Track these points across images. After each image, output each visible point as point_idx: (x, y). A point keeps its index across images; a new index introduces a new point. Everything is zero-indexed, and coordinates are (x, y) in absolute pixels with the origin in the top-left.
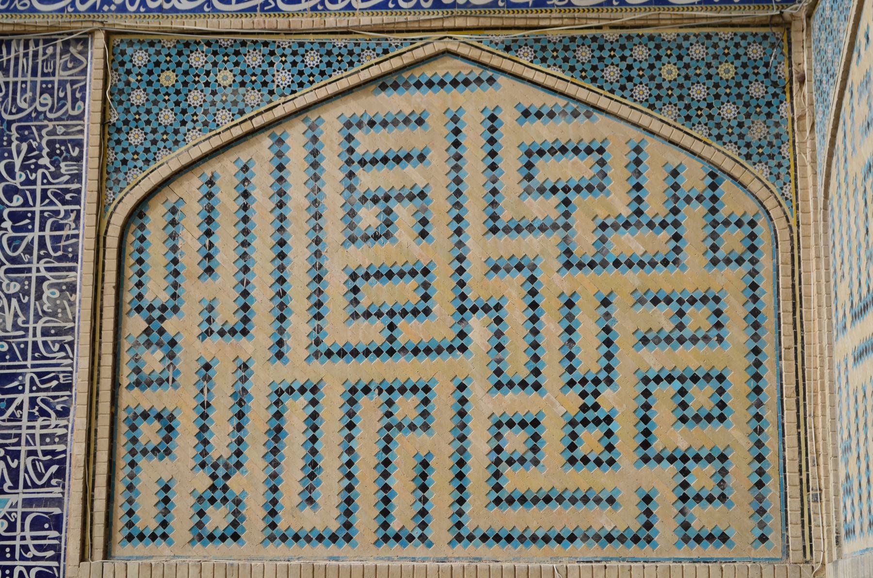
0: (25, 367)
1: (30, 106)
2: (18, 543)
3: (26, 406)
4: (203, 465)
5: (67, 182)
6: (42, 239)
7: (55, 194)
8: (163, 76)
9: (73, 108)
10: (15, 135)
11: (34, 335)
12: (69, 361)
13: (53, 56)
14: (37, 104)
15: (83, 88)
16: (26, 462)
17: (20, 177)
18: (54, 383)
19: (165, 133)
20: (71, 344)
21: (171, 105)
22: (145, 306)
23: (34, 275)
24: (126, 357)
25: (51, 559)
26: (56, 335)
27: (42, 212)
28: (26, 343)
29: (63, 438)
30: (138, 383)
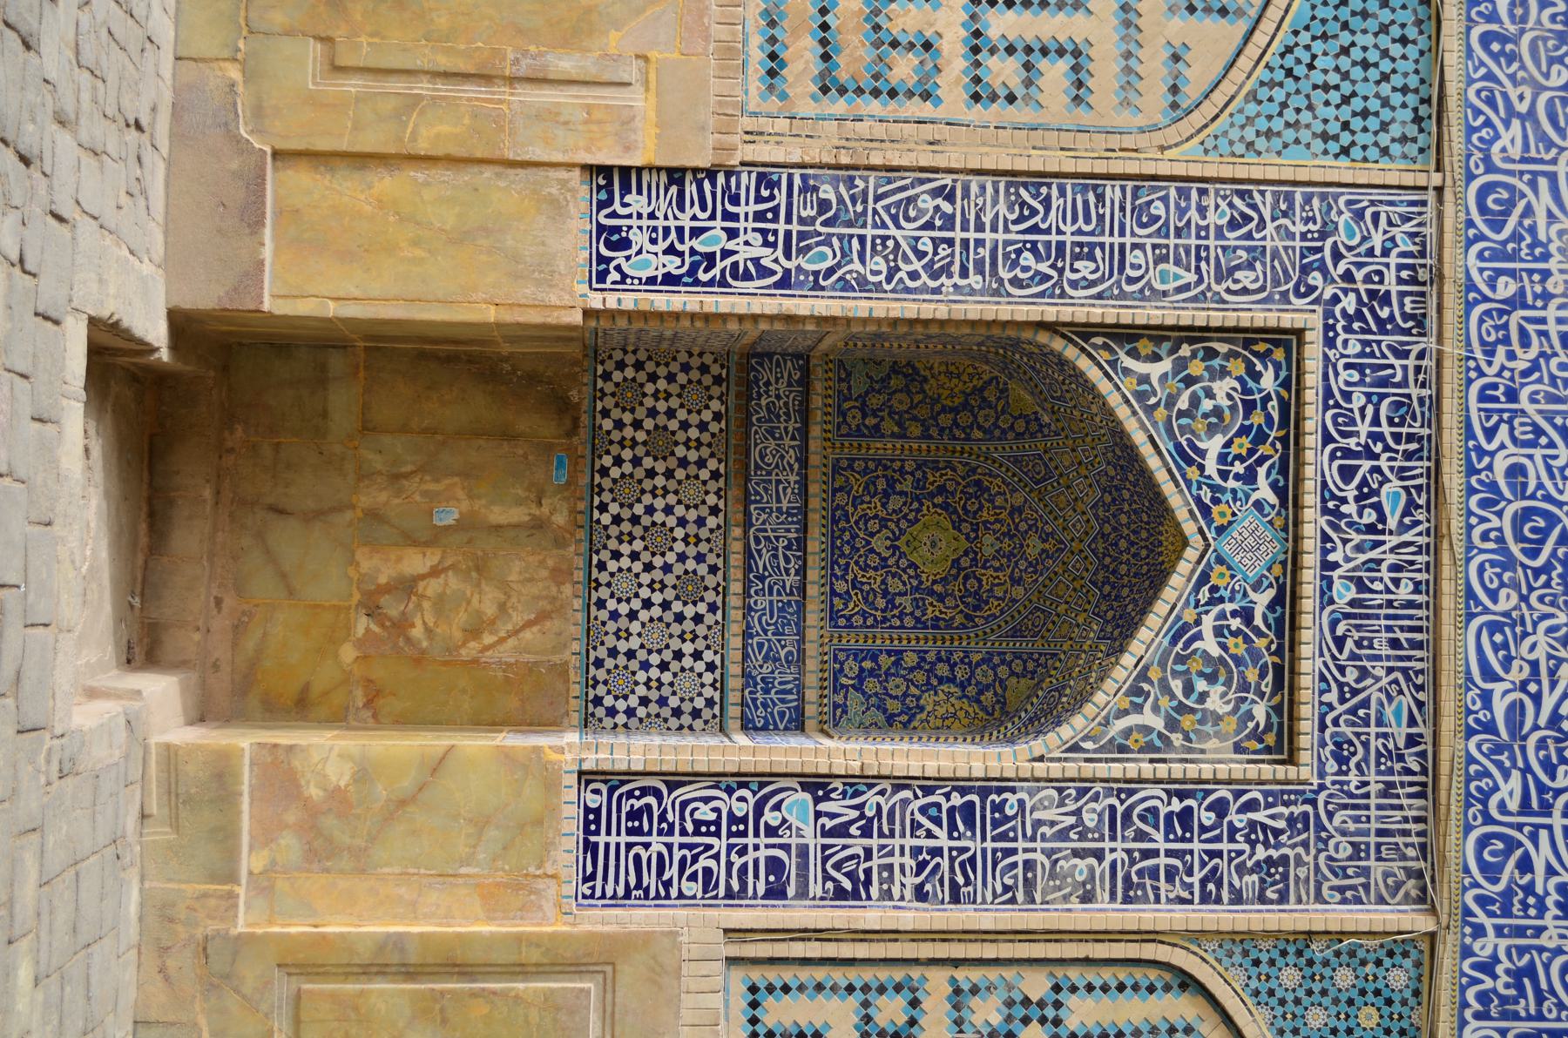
0: (984, 839)
1: (1336, 829)
2: (750, 840)
3: (932, 843)
5: (1231, 884)
6: (1155, 853)
7: (1215, 869)
8: (1373, 1011)
9: (1332, 888)
10: (1297, 810)
11: (1026, 850)
12: (989, 898)
13: (1404, 858)
14: (1338, 838)
15: (1359, 901)
16: (857, 845)
17: (1239, 820)
18: (960, 880)
19: (1294, 1016)
20: (1013, 901)
21: (1333, 1023)
22: (1060, 997)
23: (1107, 845)
24: (993, 974)
25: (728, 887)
26: (1026, 879)
27: (1191, 852)
28: (1015, 839)
29: (888, 895)
30: (957, 991)
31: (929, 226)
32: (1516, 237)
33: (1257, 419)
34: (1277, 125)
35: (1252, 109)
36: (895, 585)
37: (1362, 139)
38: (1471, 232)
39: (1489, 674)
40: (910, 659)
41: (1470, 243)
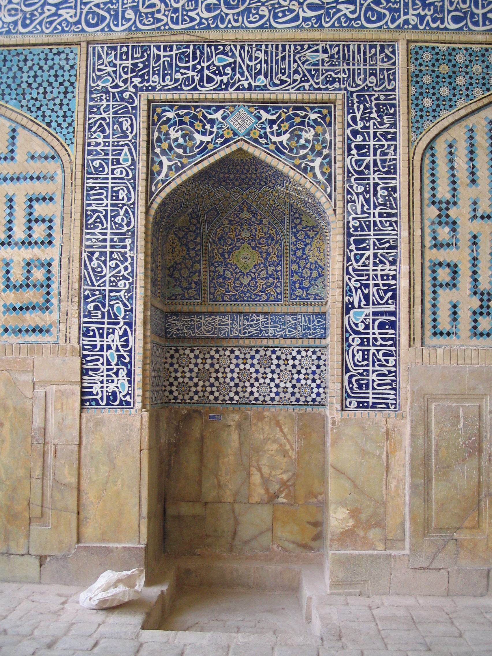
0: (369, 235)
1: (364, 83)
2: (371, 336)
3: (371, 258)
4: (475, 293)
5: (388, 128)
6: (375, 161)
7: (381, 135)
8: (441, 67)
9: (389, 85)
10: (356, 100)
11: (374, 217)
12: (395, 232)
13: (375, 54)
14: (367, 82)
15: (394, 74)
16: (373, 290)
17: (360, 124)
18: (387, 245)
19: (444, 101)
20: (396, 222)
21: (446, 84)
22: (437, 201)
23: (371, 182)
24: (427, 231)
25: (391, 345)
26: (387, 217)
27: (374, 145)
28: (369, 221)
29: (394, 277)
30: (435, 246)
31: (105, 262)
32: (108, 11)
33: (187, 119)
34: (61, 113)
35: (54, 124)
36: (263, 274)
37: (67, 77)
38: (106, 29)
39: (296, 18)
40: (295, 267)
41: (111, 30)
